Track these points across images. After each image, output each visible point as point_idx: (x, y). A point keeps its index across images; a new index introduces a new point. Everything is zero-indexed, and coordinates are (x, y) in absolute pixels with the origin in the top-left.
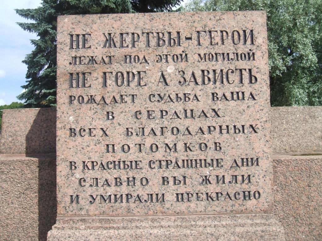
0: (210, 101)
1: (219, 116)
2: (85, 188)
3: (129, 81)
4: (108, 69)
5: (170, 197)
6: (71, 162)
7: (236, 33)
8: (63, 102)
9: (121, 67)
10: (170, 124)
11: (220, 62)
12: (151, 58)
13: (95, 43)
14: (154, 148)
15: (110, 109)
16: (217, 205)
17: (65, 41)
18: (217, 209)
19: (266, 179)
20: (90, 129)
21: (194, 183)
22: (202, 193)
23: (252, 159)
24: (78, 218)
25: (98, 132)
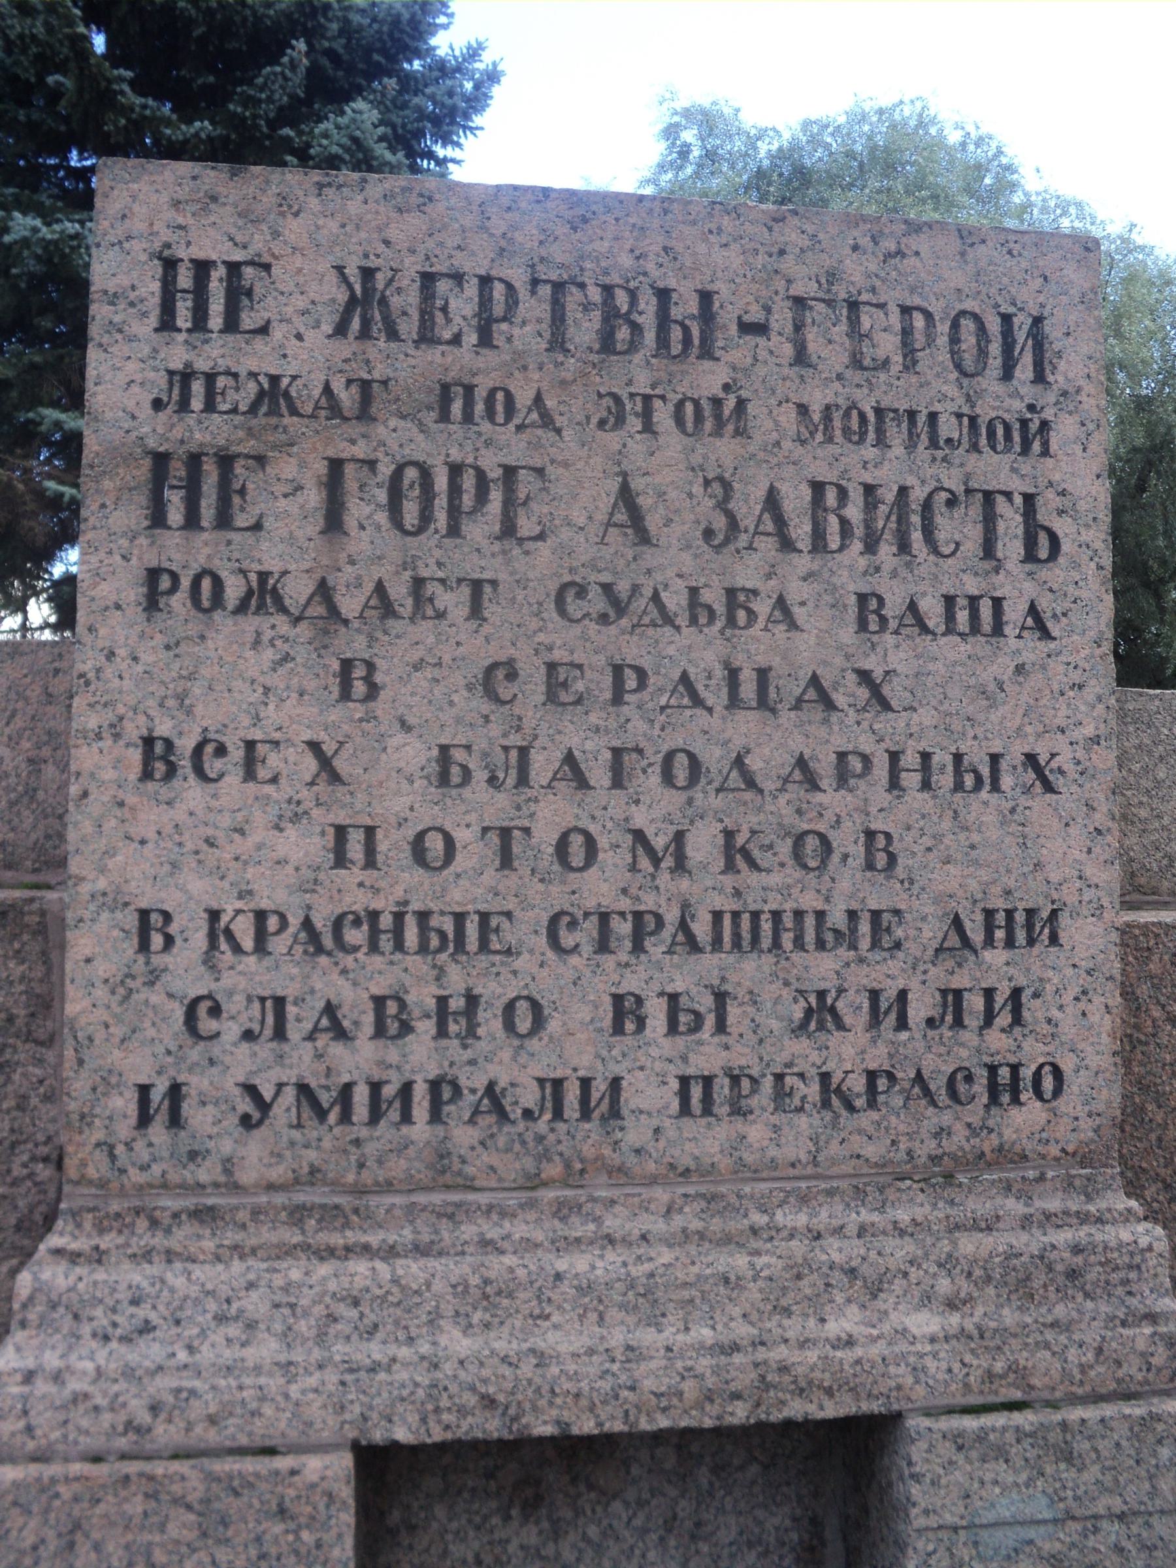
0: (847, 634)
1: (886, 706)
2: (216, 1050)
3: (454, 511)
4: (353, 442)
5: (649, 1095)
6: (144, 914)
7: (968, 325)
8: (113, 598)
9: (421, 437)
10: (657, 732)
11: (898, 450)
12: (573, 408)
13: (290, 309)
14: (575, 850)
15: (356, 645)
16: (871, 1130)
17: (133, 288)
18: (871, 1151)
19: (1089, 1008)
20: (250, 745)
21: (764, 1032)
22: (801, 1076)
23: (1030, 913)
24: (171, 1203)
25: (291, 759)
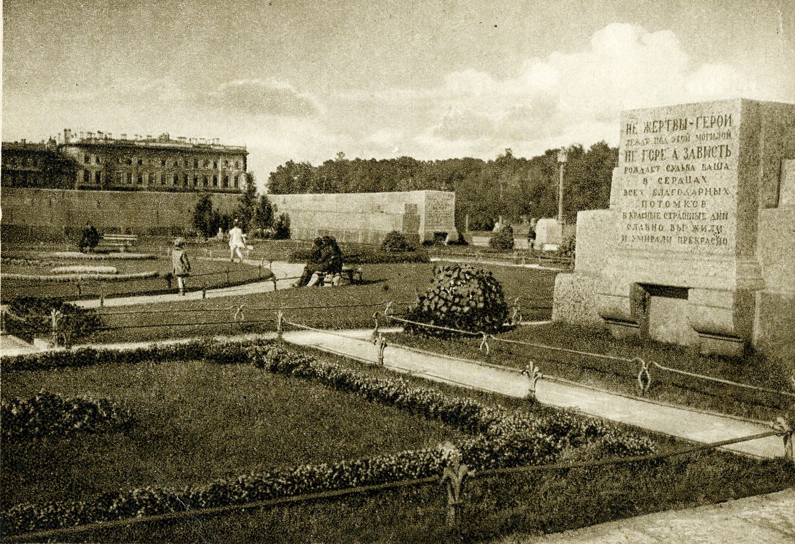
14: (667, 205)
